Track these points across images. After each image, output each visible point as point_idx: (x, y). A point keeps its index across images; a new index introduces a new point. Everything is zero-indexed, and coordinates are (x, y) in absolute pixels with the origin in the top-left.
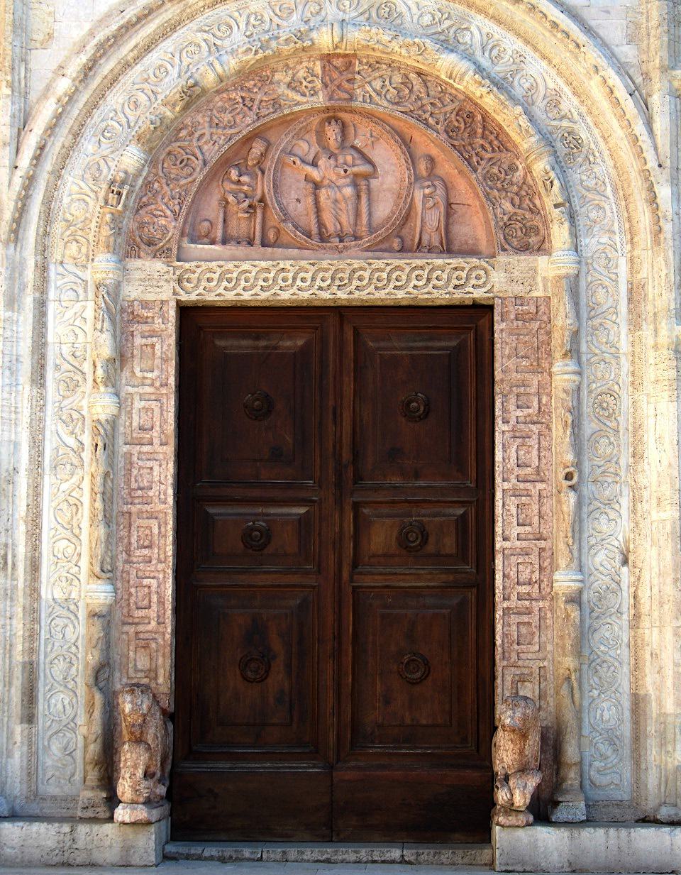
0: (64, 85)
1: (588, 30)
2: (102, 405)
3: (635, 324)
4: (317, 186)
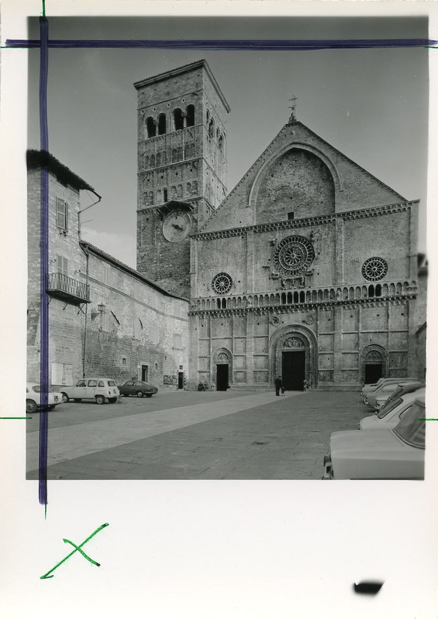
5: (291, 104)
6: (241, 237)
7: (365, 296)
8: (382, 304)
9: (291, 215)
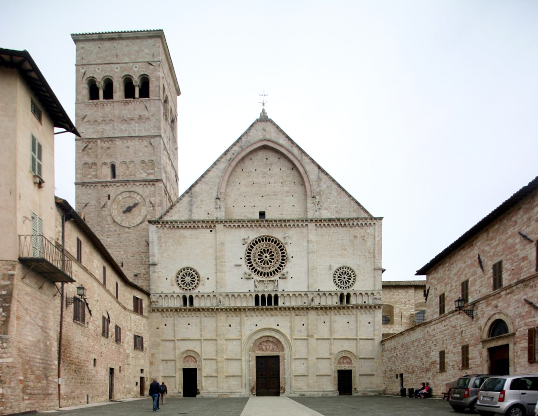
5: (261, 99)
6: (209, 230)
7: (337, 303)
8: (352, 312)
9: (262, 214)
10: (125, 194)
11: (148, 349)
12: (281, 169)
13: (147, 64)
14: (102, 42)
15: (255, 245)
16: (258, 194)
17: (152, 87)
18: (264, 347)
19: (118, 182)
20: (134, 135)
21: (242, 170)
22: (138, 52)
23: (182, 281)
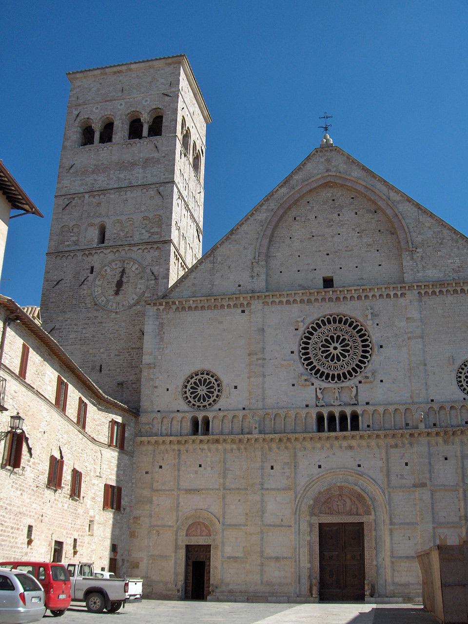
0: (302, 492)
1: (375, 482)
2: (308, 538)
3: (384, 525)
4: (338, 505)
9: (328, 283)
10: (116, 264)
11: (128, 509)
12: (356, 214)
13: (162, 95)
14: (105, 77)
15: (316, 330)
16: (320, 251)
17: (165, 123)
18: (335, 507)
19: (107, 248)
20: (136, 184)
21: (295, 219)
22: (151, 83)
23: (192, 393)
